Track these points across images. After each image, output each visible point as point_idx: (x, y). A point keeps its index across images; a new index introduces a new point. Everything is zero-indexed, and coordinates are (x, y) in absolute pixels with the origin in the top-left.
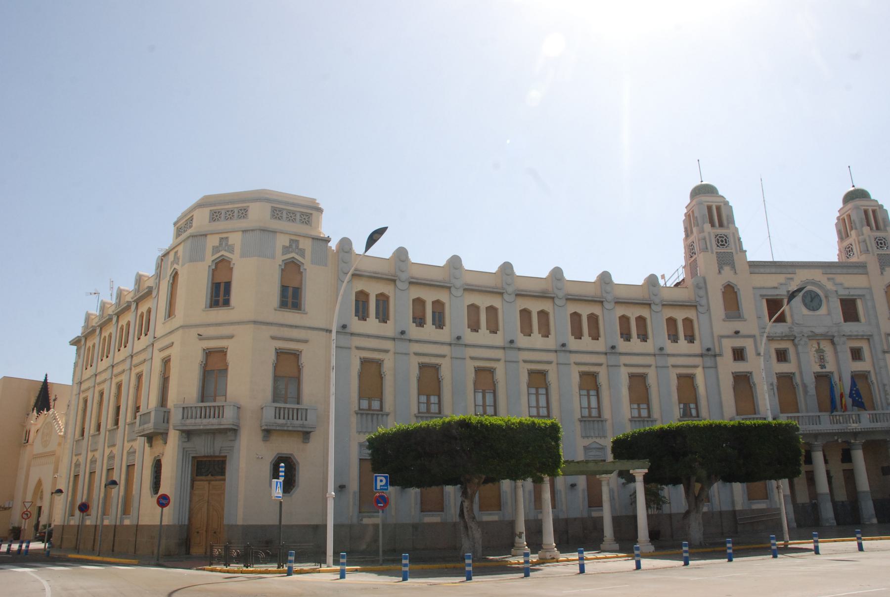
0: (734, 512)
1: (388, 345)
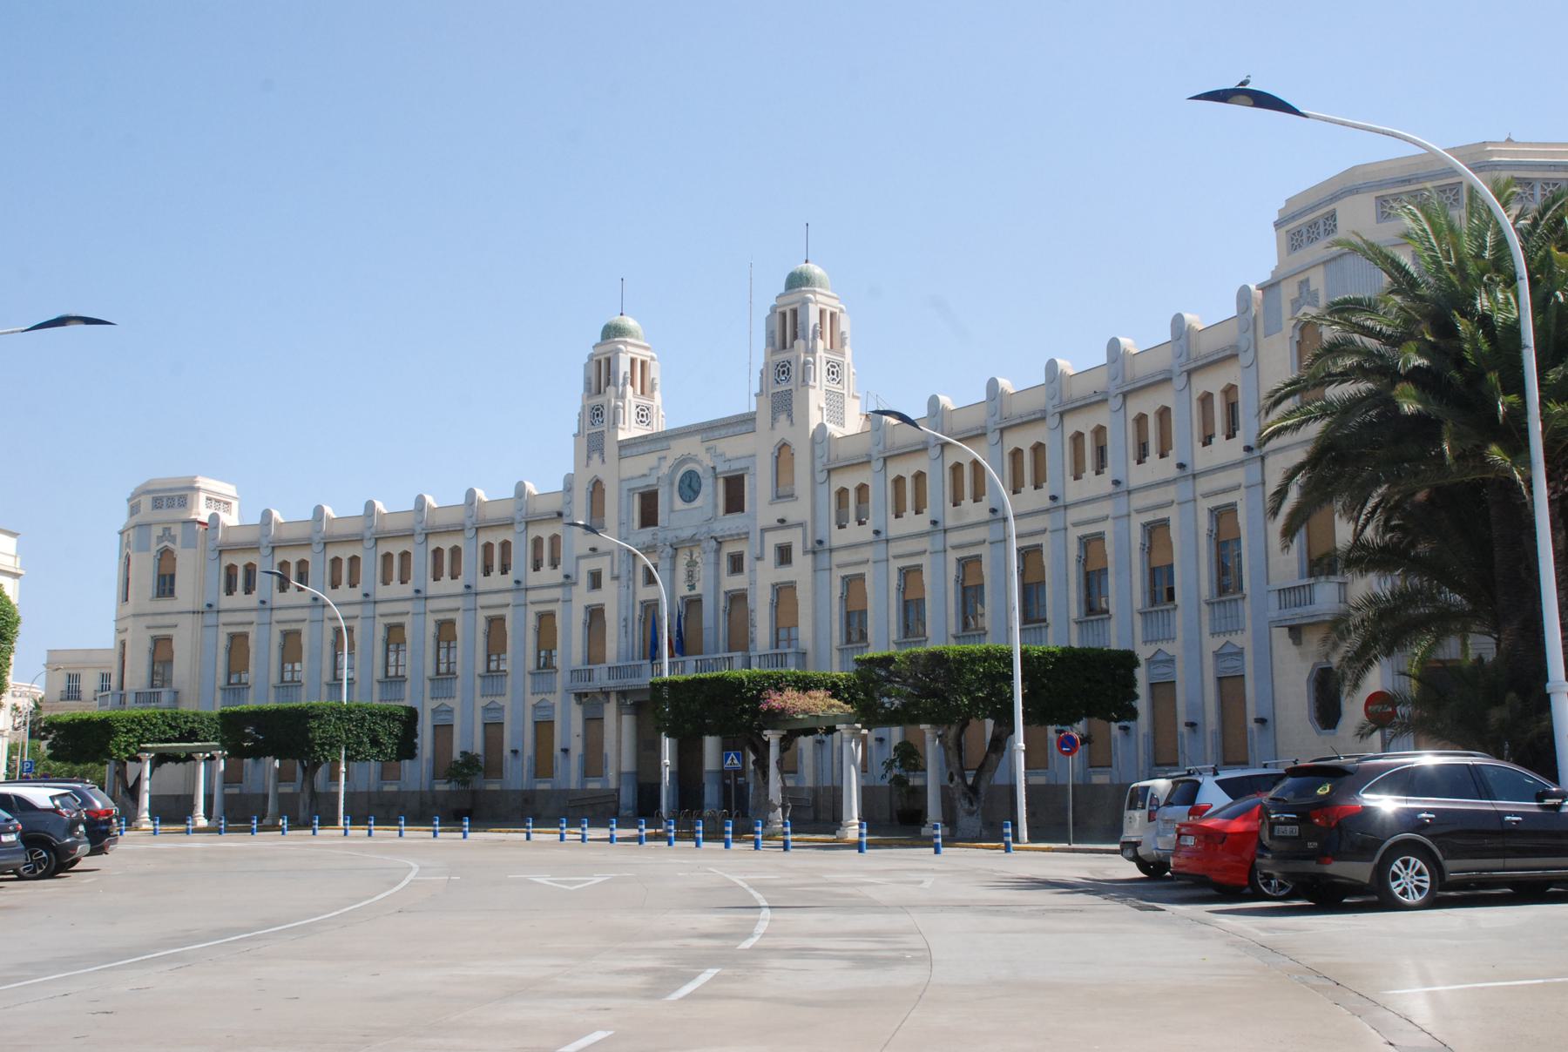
0: (567, 791)
1: (253, 616)
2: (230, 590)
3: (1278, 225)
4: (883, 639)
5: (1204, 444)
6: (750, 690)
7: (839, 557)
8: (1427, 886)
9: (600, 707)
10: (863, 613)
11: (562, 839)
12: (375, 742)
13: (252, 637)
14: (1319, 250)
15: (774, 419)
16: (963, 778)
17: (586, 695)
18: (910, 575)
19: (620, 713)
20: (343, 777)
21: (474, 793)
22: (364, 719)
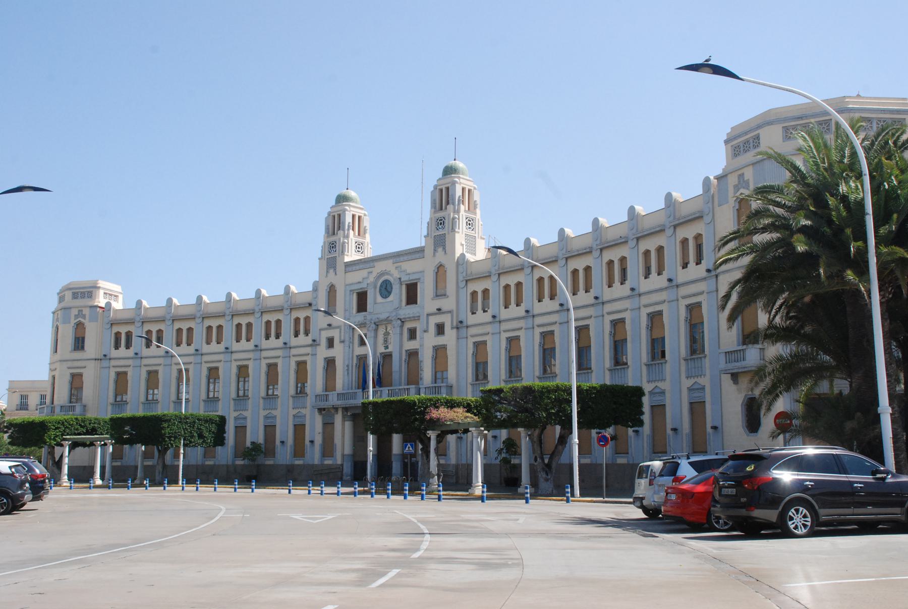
0: (313, 466)
1: (130, 362)
2: (117, 347)
3: (726, 142)
4: (497, 378)
5: (683, 268)
6: (420, 407)
7: (472, 331)
8: (809, 524)
9: (332, 416)
10: (486, 363)
11: (309, 493)
12: (201, 436)
13: (129, 374)
14: (749, 157)
15: (435, 250)
16: (543, 459)
17: (324, 409)
18: (513, 341)
19: (344, 418)
20: (182, 456)
21: (258, 466)
22: (194, 422)
